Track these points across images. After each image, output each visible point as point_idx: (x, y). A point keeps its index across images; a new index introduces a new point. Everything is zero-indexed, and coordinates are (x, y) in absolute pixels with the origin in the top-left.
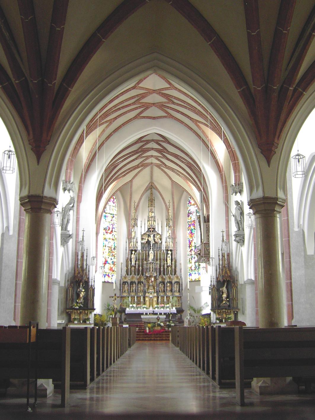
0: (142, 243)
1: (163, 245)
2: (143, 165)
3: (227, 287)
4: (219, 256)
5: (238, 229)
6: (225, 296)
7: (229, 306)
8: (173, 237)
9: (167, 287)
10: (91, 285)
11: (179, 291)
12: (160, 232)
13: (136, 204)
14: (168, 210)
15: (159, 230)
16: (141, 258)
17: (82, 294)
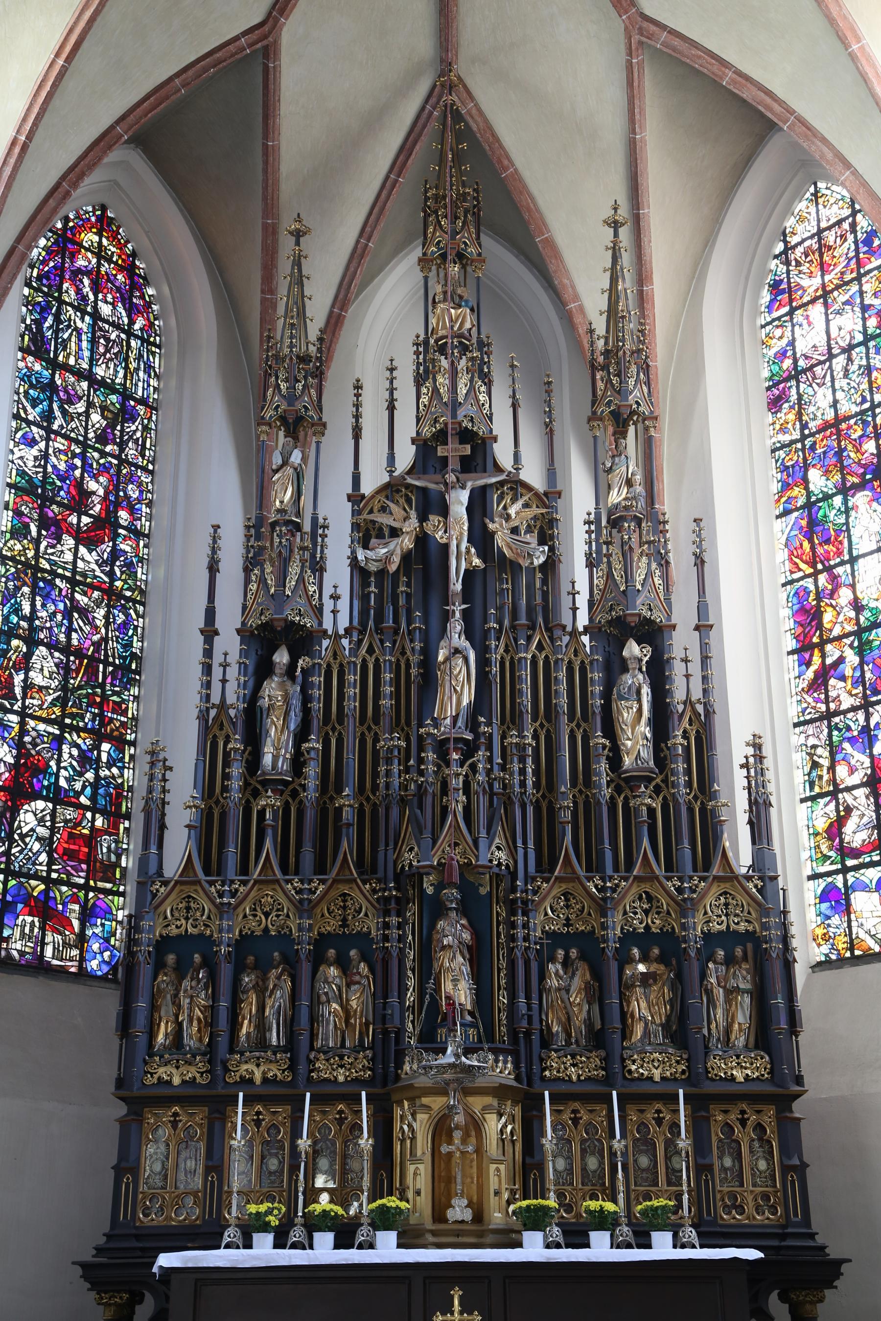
1: (565, 587)
9: (625, 988)
12: (533, 474)
15: (518, 450)
16: (352, 705)
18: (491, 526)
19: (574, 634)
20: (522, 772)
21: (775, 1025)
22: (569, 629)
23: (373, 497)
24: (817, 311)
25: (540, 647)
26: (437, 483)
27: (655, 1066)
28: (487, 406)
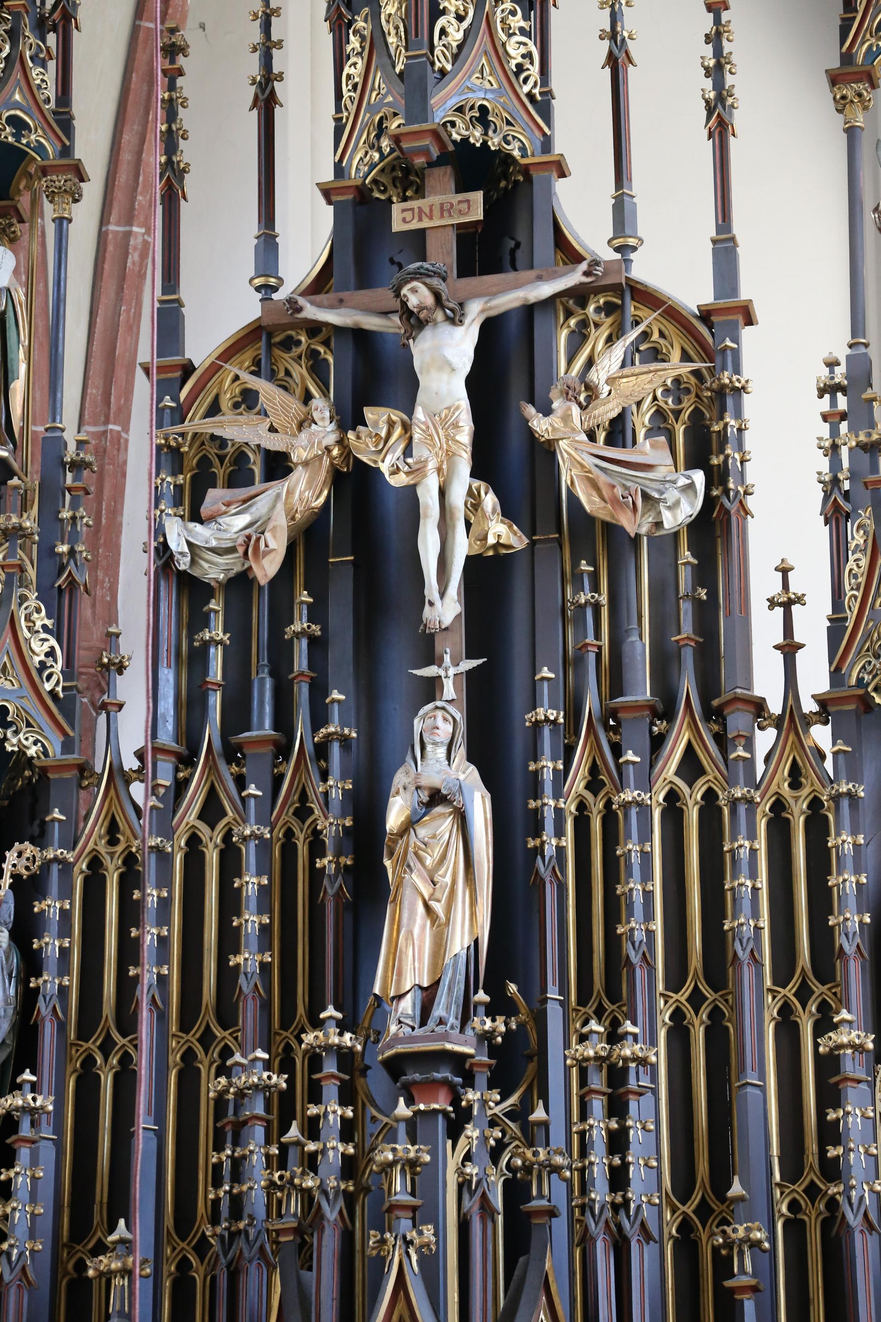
0: (182, 586)
1: (762, 584)
18: (540, 425)
19: (792, 721)
20: (618, 1142)
22: (775, 707)
23: (214, 369)
25: (691, 767)
26: (385, 313)
28: (534, 70)
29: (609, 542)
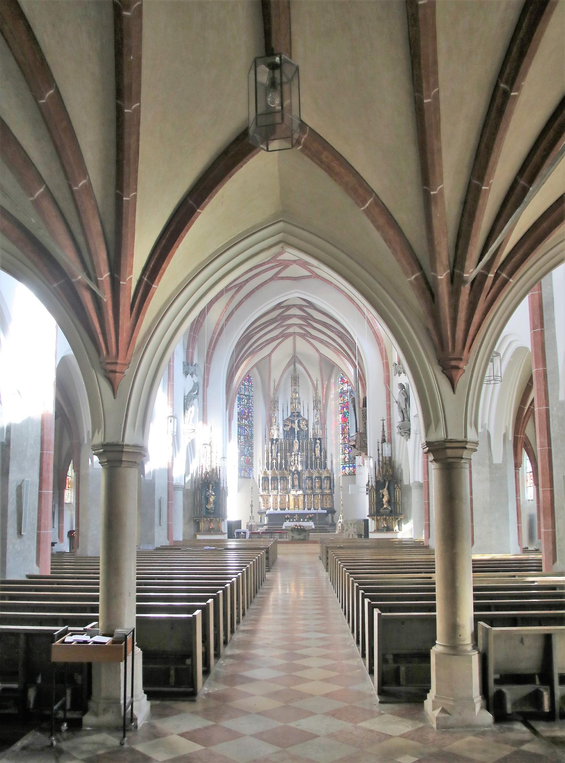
2: (284, 336)
3: (388, 489)
4: (378, 450)
5: (402, 419)
6: (385, 500)
7: (391, 511)
8: (322, 422)
9: (315, 482)
10: (223, 488)
11: (330, 488)
13: (276, 383)
14: (316, 389)
17: (212, 499)
21: (331, 488)
24: (346, 384)
27: (318, 491)
29: (302, 430)
